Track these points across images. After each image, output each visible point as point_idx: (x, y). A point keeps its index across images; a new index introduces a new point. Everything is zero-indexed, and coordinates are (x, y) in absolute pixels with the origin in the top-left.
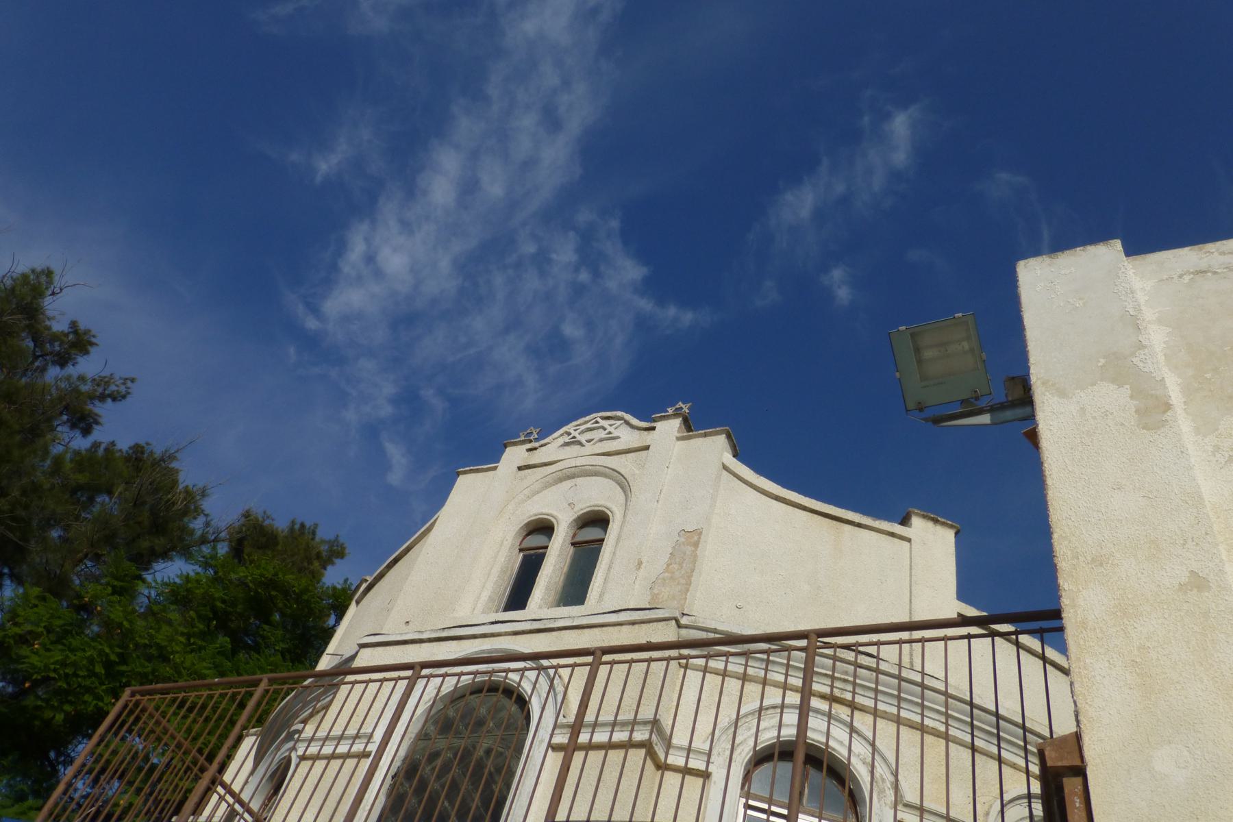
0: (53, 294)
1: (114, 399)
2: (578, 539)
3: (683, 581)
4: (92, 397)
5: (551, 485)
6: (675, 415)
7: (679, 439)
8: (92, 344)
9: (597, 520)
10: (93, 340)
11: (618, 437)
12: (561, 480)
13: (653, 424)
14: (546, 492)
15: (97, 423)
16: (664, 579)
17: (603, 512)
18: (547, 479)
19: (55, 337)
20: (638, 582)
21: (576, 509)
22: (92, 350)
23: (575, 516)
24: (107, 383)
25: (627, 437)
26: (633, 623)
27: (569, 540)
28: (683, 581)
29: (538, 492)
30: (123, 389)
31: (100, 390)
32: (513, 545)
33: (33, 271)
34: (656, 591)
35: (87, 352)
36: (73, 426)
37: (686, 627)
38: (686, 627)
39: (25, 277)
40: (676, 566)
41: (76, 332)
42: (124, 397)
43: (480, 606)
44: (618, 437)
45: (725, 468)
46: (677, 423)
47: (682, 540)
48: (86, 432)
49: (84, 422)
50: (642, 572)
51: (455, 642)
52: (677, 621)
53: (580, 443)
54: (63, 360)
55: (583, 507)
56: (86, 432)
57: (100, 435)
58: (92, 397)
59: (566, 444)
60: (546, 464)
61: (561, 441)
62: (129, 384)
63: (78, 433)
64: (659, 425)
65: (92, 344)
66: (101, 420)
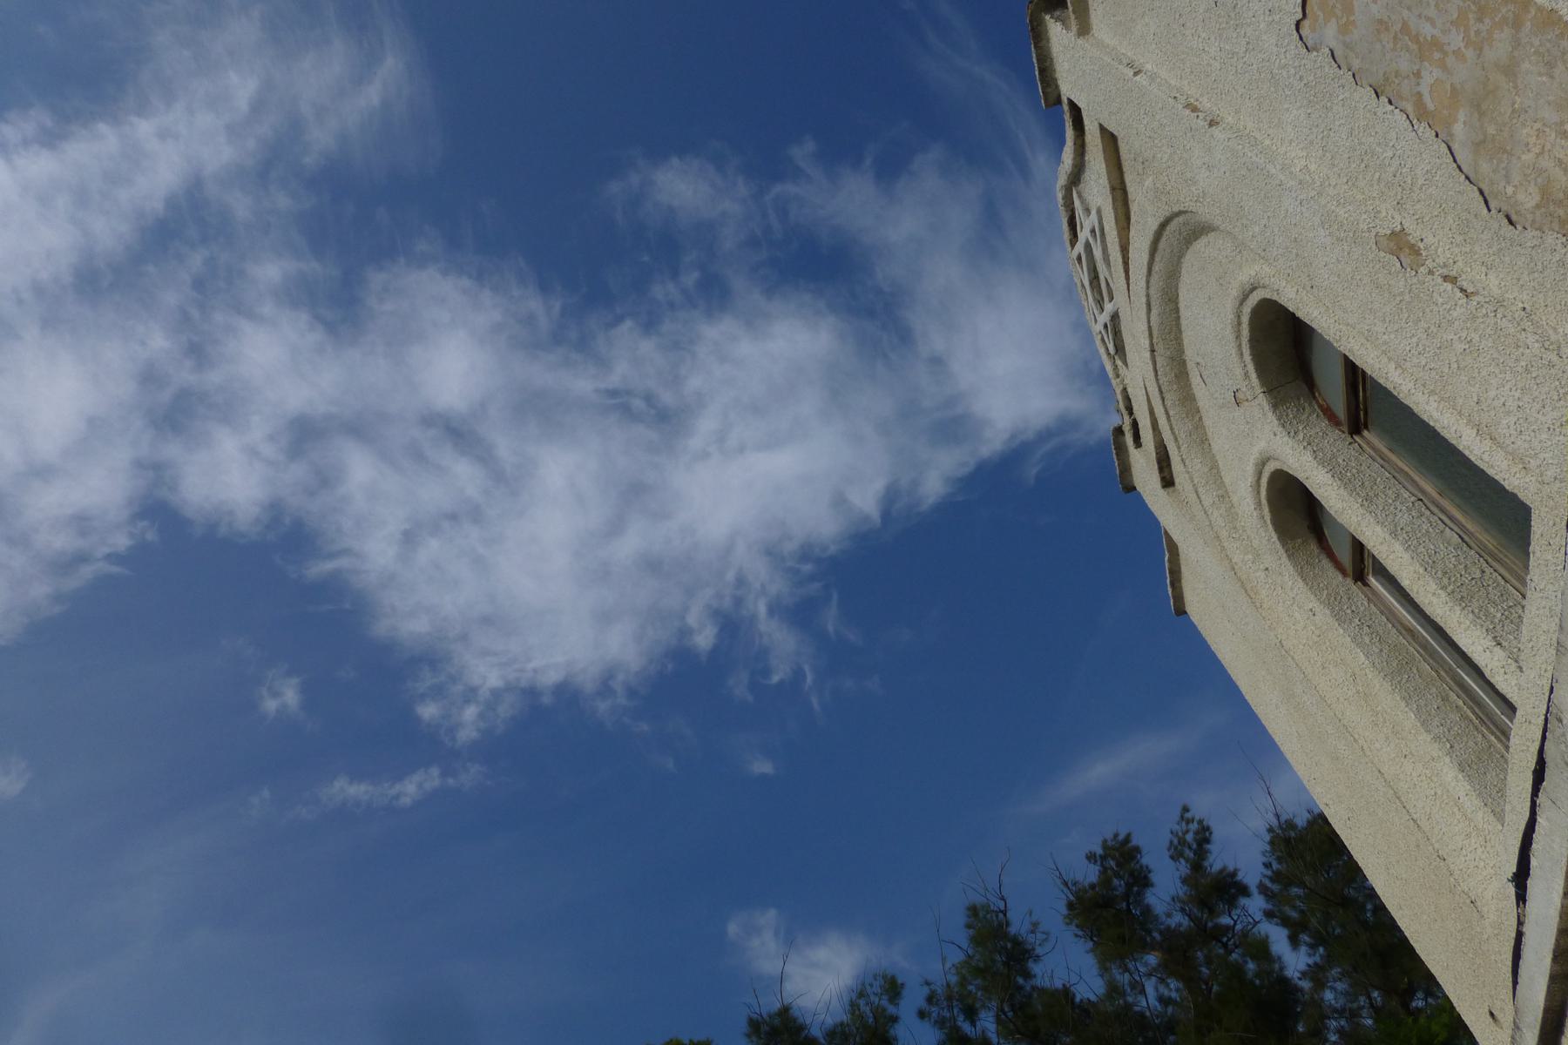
1: (1207, 841)
2: (1340, 410)
3: (1500, 48)
4: (1197, 866)
5: (1199, 426)
6: (1038, 35)
8: (1128, 839)
10: (1121, 837)
12: (1188, 398)
13: (1065, 101)
14: (1215, 447)
15: (1234, 874)
16: (1478, 146)
18: (1182, 436)
19: (1105, 881)
22: (1135, 842)
23: (1262, 400)
24: (1182, 842)
27: (1336, 440)
29: (1214, 466)
30: (1194, 826)
32: (1334, 603)
33: (968, 926)
34: (1528, 199)
35: (1137, 850)
36: (1232, 903)
39: (977, 941)
40: (1430, 75)
41: (1103, 858)
42: (1208, 829)
43: (1482, 817)
47: (1330, 34)
48: (1244, 891)
49: (1228, 889)
50: (1440, 245)
53: (1115, 317)
54: (1142, 880)
56: (1244, 891)
58: (1197, 866)
60: (1152, 413)
61: (1119, 362)
62: (1188, 815)
63: (1243, 901)
64: (1067, 90)
65: (1128, 839)
66: (1231, 868)
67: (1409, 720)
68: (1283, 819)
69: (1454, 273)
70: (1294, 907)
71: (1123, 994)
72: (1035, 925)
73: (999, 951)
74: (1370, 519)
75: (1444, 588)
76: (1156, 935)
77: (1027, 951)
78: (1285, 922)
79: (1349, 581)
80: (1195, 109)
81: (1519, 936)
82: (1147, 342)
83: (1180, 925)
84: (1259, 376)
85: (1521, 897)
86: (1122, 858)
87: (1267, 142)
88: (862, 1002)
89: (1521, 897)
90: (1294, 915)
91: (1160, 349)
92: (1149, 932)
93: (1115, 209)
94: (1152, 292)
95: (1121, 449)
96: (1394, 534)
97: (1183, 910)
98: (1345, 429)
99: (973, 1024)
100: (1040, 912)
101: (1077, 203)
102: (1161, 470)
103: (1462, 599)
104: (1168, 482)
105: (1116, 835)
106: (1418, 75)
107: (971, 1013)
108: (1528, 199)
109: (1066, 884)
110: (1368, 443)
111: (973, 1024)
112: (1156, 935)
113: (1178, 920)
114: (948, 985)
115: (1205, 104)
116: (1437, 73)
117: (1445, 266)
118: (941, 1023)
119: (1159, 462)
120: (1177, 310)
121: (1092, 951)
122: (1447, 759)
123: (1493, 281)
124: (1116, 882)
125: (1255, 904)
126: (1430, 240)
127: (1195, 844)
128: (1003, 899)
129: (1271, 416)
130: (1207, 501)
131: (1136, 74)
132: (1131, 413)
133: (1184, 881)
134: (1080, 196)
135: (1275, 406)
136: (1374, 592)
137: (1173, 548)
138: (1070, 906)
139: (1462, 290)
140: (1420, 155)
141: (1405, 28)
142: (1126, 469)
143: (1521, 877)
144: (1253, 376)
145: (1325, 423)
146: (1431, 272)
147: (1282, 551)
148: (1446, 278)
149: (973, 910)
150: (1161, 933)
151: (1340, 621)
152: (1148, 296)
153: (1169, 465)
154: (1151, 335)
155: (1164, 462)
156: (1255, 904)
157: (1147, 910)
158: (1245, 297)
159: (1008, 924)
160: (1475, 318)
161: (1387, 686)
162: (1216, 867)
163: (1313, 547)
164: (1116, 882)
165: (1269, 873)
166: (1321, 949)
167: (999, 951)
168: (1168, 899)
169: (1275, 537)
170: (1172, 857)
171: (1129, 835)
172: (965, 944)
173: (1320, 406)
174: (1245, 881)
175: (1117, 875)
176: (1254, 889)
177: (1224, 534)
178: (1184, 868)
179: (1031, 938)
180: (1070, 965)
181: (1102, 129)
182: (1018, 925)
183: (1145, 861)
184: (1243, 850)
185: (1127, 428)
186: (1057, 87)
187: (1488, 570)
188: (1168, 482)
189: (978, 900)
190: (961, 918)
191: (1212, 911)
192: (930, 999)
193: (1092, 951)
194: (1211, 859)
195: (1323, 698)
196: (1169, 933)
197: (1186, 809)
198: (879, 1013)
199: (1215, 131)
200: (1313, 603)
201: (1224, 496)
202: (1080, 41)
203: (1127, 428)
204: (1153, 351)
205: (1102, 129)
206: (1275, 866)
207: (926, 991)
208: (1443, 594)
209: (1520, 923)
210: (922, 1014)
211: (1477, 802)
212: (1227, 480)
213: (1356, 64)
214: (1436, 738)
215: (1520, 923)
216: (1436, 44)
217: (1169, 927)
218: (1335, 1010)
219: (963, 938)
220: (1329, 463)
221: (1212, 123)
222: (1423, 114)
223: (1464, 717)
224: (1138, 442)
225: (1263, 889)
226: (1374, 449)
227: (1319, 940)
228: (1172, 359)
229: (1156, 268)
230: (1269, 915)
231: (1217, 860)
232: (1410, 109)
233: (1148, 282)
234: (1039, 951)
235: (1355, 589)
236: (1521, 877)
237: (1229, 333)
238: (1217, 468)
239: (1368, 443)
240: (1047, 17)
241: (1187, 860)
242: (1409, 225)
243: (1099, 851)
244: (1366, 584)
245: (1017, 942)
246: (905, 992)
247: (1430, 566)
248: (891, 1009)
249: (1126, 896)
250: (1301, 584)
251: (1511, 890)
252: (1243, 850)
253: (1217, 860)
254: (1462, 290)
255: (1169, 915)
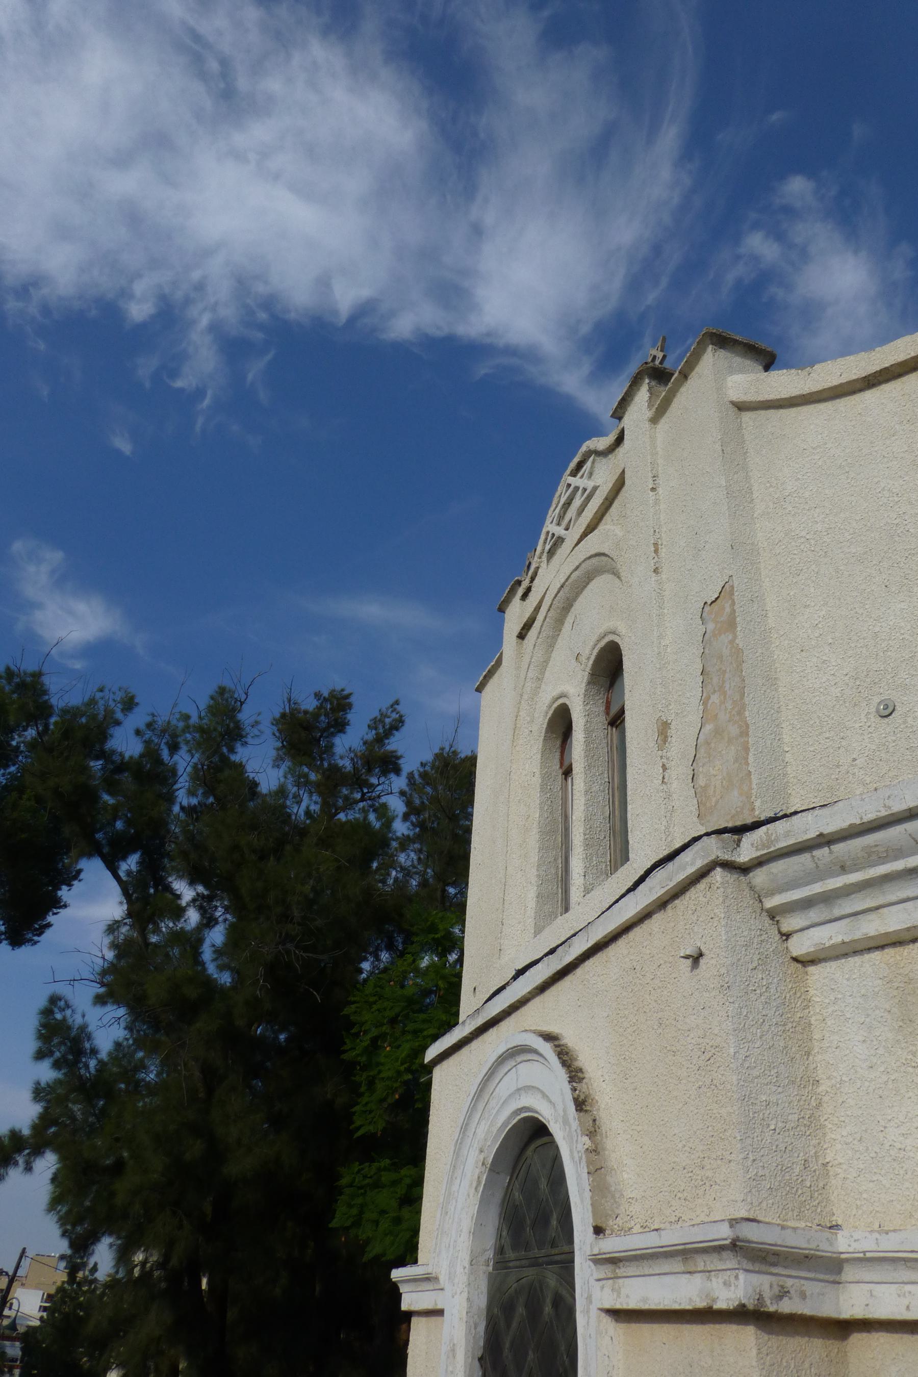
0: (242, 703)
1: (397, 729)
4: (380, 740)
6: (635, 382)
7: (654, 420)
8: (348, 696)
9: (609, 667)
10: (345, 693)
11: (595, 488)
12: (560, 622)
14: (553, 655)
15: (398, 758)
17: (603, 650)
18: (544, 634)
19: (316, 715)
20: (672, 773)
21: (583, 659)
22: (352, 699)
24: (381, 721)
25: (601, 476)
26: (663, 904)
27: (601, 720)
28: (734, 730)
29: (547, 661)
31: (381, 731)
32: (546, 777)
35: (350, 706)
36: (385, 773)
37: (759, 863)
38: (759, 863)
39: (210, 707)
44: (595, 488)
45: (741, 407)
46: (643, 395)
48: (397, 771)
49: (390, 764)
51: (492, 1033)
52: (728, 866)
54: (340, 726)
55: (589, 652)
56: (397, 771)
57: (411, 763)
58: (380, 740)
59: (551, 553)
63: (393, 776)
65: (348, 696)
66: (399, 754)
67: (534, 857)
68: (453, 749)
69: (667, 766)
70: (421, 797)
71: (286, 798)
72: (257, 723)
73: (222, 727)
74: (583, 775)
75: (585, 834)
76: (326, 764)
77: (242, 736)
78: (409, 803)
79: (560, 771)
80: (656, 551)
81: (503, 988)
82: (563, 581)
83: (344, 767)
84: (593, 665)
85: (515, 978)
86: (337, 708)
87: (666, 611)
88: (101, 702)
89: (515, 978)
90: (417, 802)
91: (566, 589)
92: (322, 760)
93: (600, 508)
94: (583, 565)
95: (513, 591)
96: (586, 792)
97: (352, 759)
98: (609, 720)
99: (171, 755)
100: (260, 713)
101: (589, 464)
102: (523, 628)
103: (587, 846)
104: (521, 636)
105: (343, 690)
106: (715, 691)
107: (174, 748)
108: (701, 781)
109: (289, 701)
110: (612, 735)
111: (171, 755)
112: (326, 764)
113: (346, 764)
114: (169, 722)
115: (663, 552)
116: (717, 701)
117: (668, 759)
118: (148, 743)
119: (525, 625)
120: (588, 584)
121: (278, 749)
122: (535, 888)
123: (675, 785)
124: (323, 718)
125: (399, 783)
126: (674, 740)
127: (388, 725)
128: (246, 694)
129: (584, 685)
130: (531, 674)
131: (653, 489)
132: (532, 579)
133: (365, 743)
134: (593, 462)
135: (589, 683)
136: (566, 785)
137: (499, 663)
138: (283, 715)
139: (663, 778)
140: (694, 717)
141: (725, 671)
142: (507, 601)
143: (520, 972)
144: (591, 662)
145: (603, 708)
146: (661, 757)
147: (543, 734)
148: (664, 765)
149: (222, 691)
150: (330, 764)
151: (542, 791)
152: (580, 564)
153: (529, 629)
154: (567, 580)
155: (527, 626)
156: (399, 783)
157: (330, 746)
158: (614, 633)
159: (239, 711)
160: (658, 792)
161: (537, 836)
162: (389, 748)
163: (558, 743)
164: (323, 718)
165: (421, 770)
166: (418, 830)
167: (222, 727)
168: (347, 748)
169: (545, 726)
170: (369, 726)
171: (351, 694)
172: (202, 707)
173: (608, 698)
174: (402, 766)
175: (326, 715)
176: (404, 774)
177: (525, 697)
178: (371, 736)
179: (248, 729)
180: (262, 763)
181: (623, 471)
182: (245, 716)
183: (350, 716)
184: (414, 750)
185: (525, 584)
186: (624, 413)
187: (607, 838)
188: (521, 636)
189: (228, 683)
190: (210, 689)
191: (370, 771)
192: (149, 725)
193: (278, 749)
194: (392, 739)
195: (508, 815)
196: (335, 770)
197: (397, 703)
198: (109, 713)
199: (654, 577)
200: (537, 771)
201: (539, 679)
202: (647, 425)
203: (525, 584)
204: (562, 586)
205: (623, 471)
206: (428, 768)
207: (149, 719)
208: (582, 838)
209: (507, 984)
210: (138, 732)
211: (533, 915)
212: (547, 674)
213: (707, 651)
214: (538, 876)
215: (507, 984)
216: (725, 693)
217: (336, 765)
218: (401, 867)
219: (204, 702)
220: (588, 731)
221: (656, 571)
222: (705, 704)
223: (557, 874)
224: (525, 596)
225: (411, 776)
226: (612, 740)
227: (422, 825)
228: (568, 599)
229: (594, 561)
230: (402, 793)
231: (394, 744)
232: (705, 695)
233: (585, 560)
234: (249, 740)
235: (560, 777)
236: (520, 972)
237: (594, 638)
238: (548, 664)
239: (612, 735)
240: (647, 381)
241: (376, 734)
242: (672, 727)
243: (326, 694)
244: (566, 779)
245: (238, 726)
246: (136, 710)
247: (587, 820)
248: (119, 715)
249: (324, 730)
250: (539, 756)
251: (514, 973)
252: (414, 750)
253: (394, 744)
254: (663, 778)
255: (342, 758)
